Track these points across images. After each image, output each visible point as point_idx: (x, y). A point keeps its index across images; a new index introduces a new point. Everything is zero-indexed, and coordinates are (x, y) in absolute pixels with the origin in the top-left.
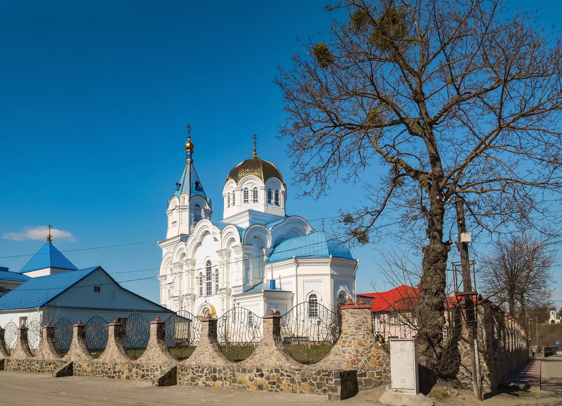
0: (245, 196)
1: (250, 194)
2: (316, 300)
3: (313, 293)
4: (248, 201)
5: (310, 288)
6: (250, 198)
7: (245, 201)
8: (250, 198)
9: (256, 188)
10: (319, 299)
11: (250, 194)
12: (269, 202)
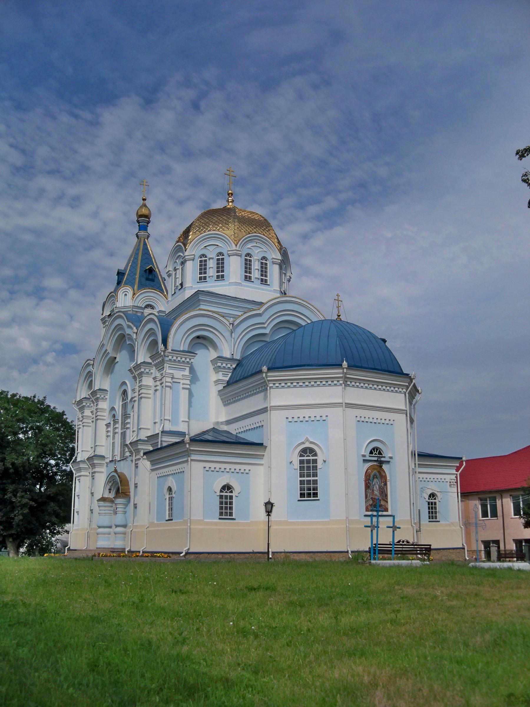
0: (200, 269)
1: (212, 264)
2: (315, 461)
3: (307, 445)
4: (205, 278)
5: (308, 436)
6: (212, 272)
7: (200, 278)
8: (212, 272)
9: (221, 254)
10: (320, 459)
11: (212, 264)
12: (248, 278)
